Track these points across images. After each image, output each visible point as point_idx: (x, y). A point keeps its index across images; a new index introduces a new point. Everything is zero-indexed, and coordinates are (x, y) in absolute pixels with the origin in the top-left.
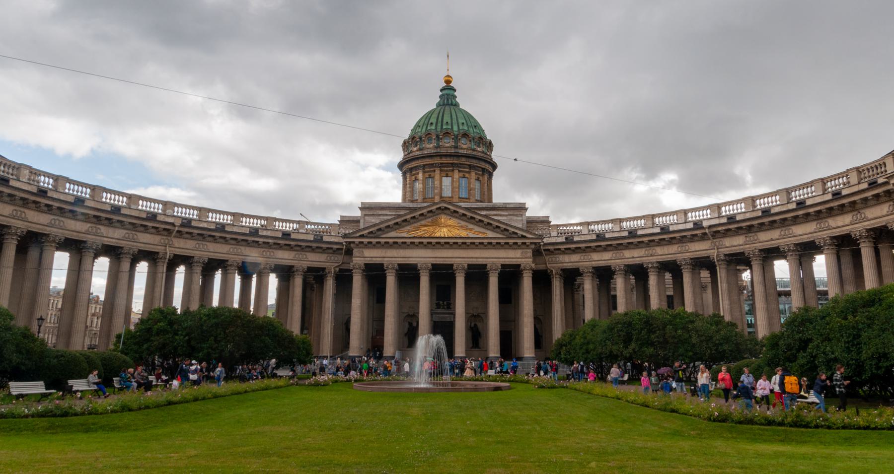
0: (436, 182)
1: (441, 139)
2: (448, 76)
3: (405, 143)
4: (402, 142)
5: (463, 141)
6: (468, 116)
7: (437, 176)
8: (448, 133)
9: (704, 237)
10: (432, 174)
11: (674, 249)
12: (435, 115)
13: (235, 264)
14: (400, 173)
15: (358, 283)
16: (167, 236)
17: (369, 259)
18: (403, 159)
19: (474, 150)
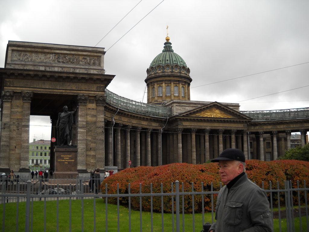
0: (172, 89)
5: (182, 70)
10: (169, 85)
19: (186, 75)
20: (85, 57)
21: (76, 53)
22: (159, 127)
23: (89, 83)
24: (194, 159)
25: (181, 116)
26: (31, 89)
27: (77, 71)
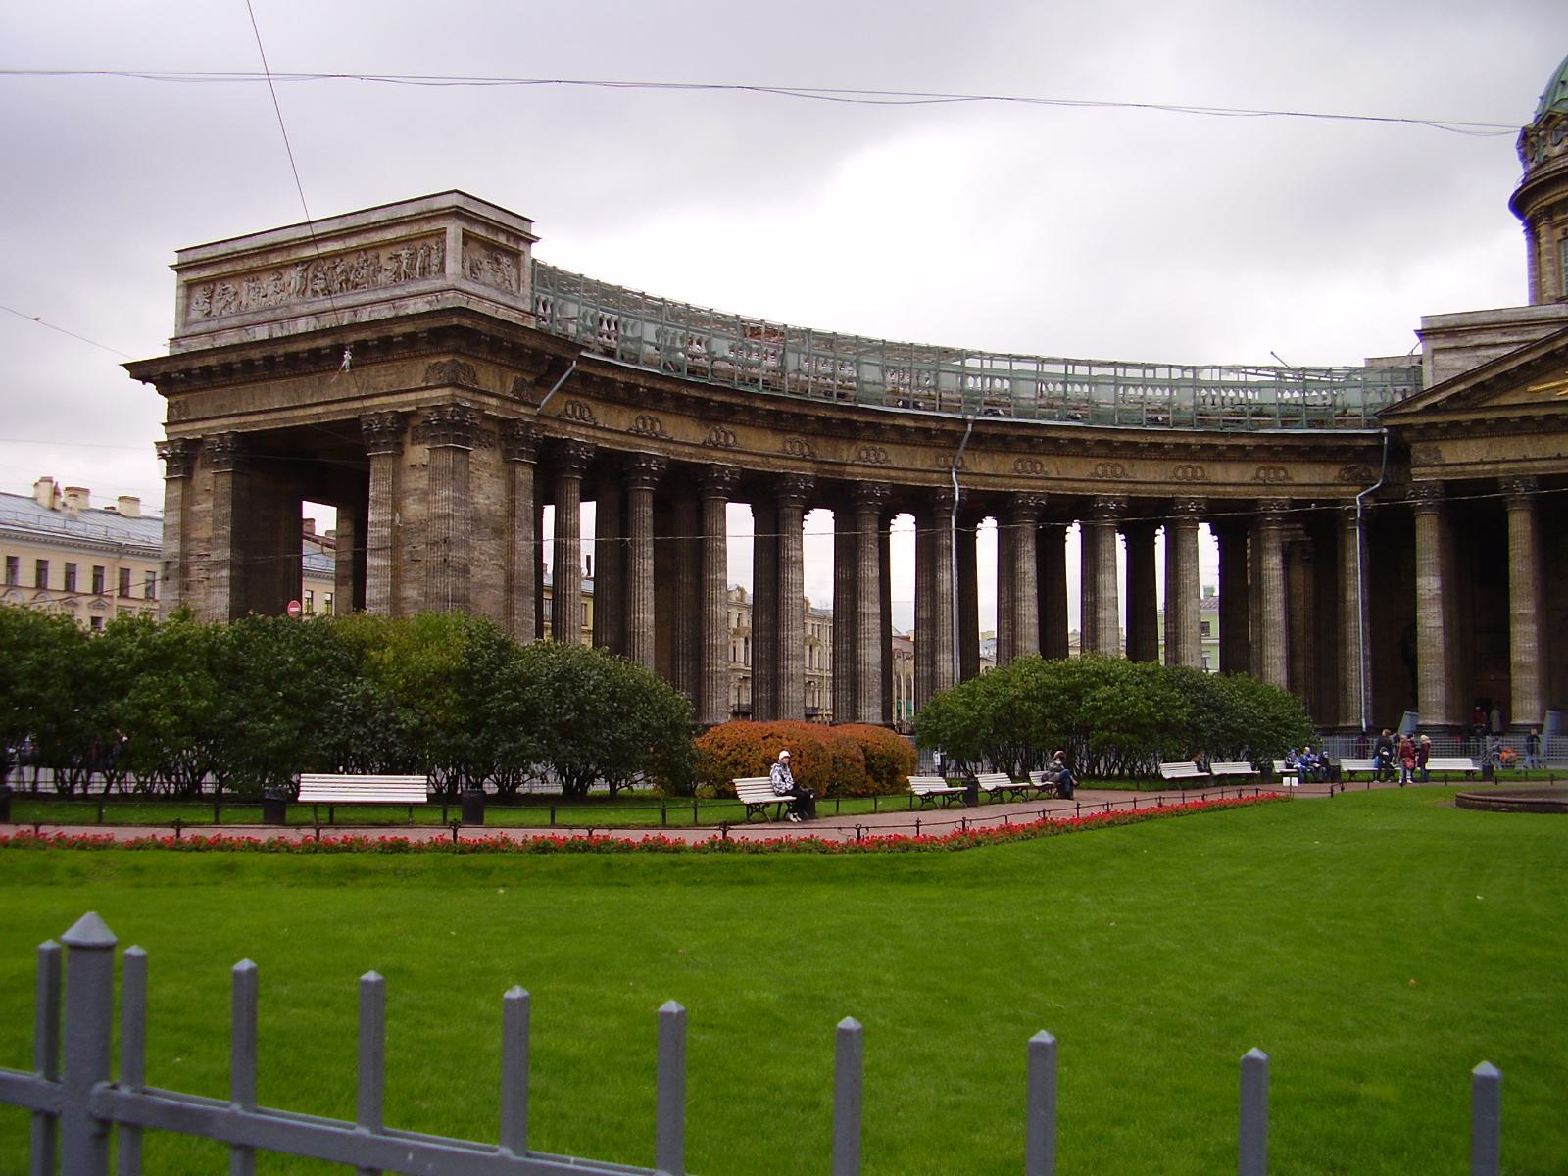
3: (1526, 136)
4: (1516, 136)
14: (1517, 227)
15: (1427, 536)
16: (948, 447)
18: (1525, 183)
20: (393, 250)
21: (364, 242)
22: (1343, 489)
23: (399, 359)
24: (1522, 666)
25: (1416, 414)
26: (224, 422)
27: (364, 316)
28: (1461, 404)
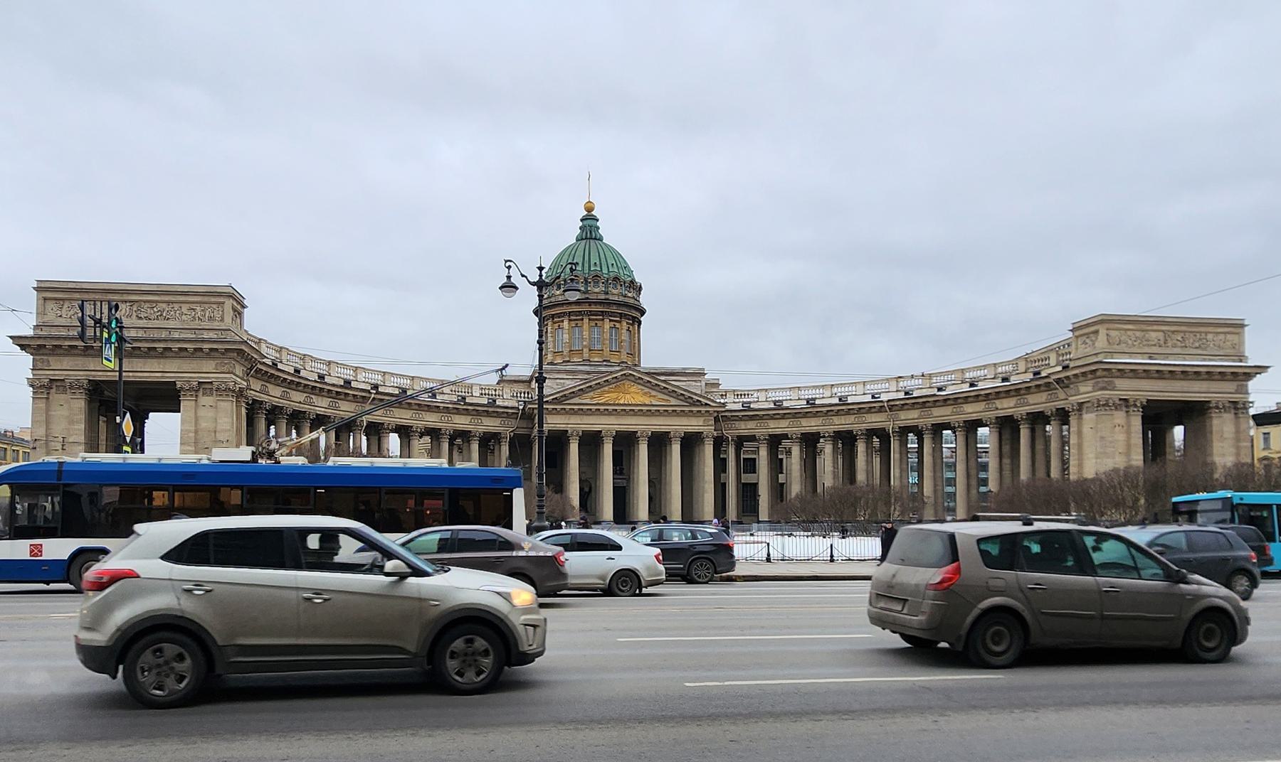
0: (584, 333)
1: (590, 283)
2: (589, 202)
6: (616, 255)
7: (586, 326)
8: (597, 276)
9: (881, 409)
11: (851, 419)
12: (579, 252)
13: (419, 430)
17: (553, 425)
28: (554, 401)
